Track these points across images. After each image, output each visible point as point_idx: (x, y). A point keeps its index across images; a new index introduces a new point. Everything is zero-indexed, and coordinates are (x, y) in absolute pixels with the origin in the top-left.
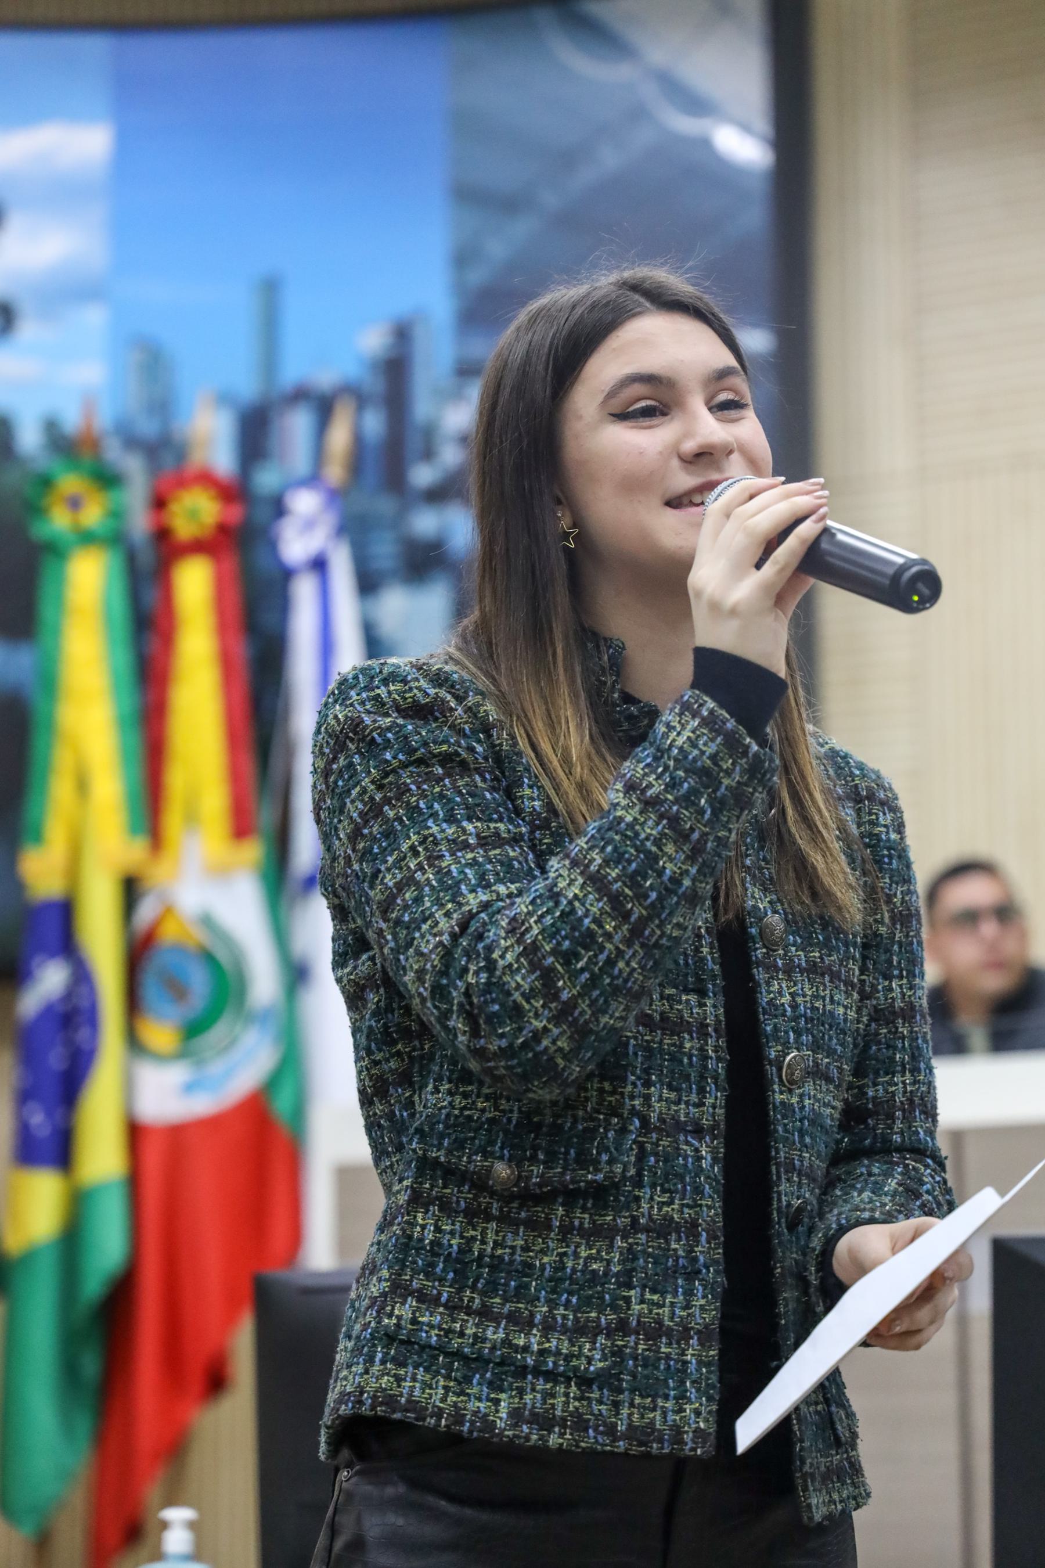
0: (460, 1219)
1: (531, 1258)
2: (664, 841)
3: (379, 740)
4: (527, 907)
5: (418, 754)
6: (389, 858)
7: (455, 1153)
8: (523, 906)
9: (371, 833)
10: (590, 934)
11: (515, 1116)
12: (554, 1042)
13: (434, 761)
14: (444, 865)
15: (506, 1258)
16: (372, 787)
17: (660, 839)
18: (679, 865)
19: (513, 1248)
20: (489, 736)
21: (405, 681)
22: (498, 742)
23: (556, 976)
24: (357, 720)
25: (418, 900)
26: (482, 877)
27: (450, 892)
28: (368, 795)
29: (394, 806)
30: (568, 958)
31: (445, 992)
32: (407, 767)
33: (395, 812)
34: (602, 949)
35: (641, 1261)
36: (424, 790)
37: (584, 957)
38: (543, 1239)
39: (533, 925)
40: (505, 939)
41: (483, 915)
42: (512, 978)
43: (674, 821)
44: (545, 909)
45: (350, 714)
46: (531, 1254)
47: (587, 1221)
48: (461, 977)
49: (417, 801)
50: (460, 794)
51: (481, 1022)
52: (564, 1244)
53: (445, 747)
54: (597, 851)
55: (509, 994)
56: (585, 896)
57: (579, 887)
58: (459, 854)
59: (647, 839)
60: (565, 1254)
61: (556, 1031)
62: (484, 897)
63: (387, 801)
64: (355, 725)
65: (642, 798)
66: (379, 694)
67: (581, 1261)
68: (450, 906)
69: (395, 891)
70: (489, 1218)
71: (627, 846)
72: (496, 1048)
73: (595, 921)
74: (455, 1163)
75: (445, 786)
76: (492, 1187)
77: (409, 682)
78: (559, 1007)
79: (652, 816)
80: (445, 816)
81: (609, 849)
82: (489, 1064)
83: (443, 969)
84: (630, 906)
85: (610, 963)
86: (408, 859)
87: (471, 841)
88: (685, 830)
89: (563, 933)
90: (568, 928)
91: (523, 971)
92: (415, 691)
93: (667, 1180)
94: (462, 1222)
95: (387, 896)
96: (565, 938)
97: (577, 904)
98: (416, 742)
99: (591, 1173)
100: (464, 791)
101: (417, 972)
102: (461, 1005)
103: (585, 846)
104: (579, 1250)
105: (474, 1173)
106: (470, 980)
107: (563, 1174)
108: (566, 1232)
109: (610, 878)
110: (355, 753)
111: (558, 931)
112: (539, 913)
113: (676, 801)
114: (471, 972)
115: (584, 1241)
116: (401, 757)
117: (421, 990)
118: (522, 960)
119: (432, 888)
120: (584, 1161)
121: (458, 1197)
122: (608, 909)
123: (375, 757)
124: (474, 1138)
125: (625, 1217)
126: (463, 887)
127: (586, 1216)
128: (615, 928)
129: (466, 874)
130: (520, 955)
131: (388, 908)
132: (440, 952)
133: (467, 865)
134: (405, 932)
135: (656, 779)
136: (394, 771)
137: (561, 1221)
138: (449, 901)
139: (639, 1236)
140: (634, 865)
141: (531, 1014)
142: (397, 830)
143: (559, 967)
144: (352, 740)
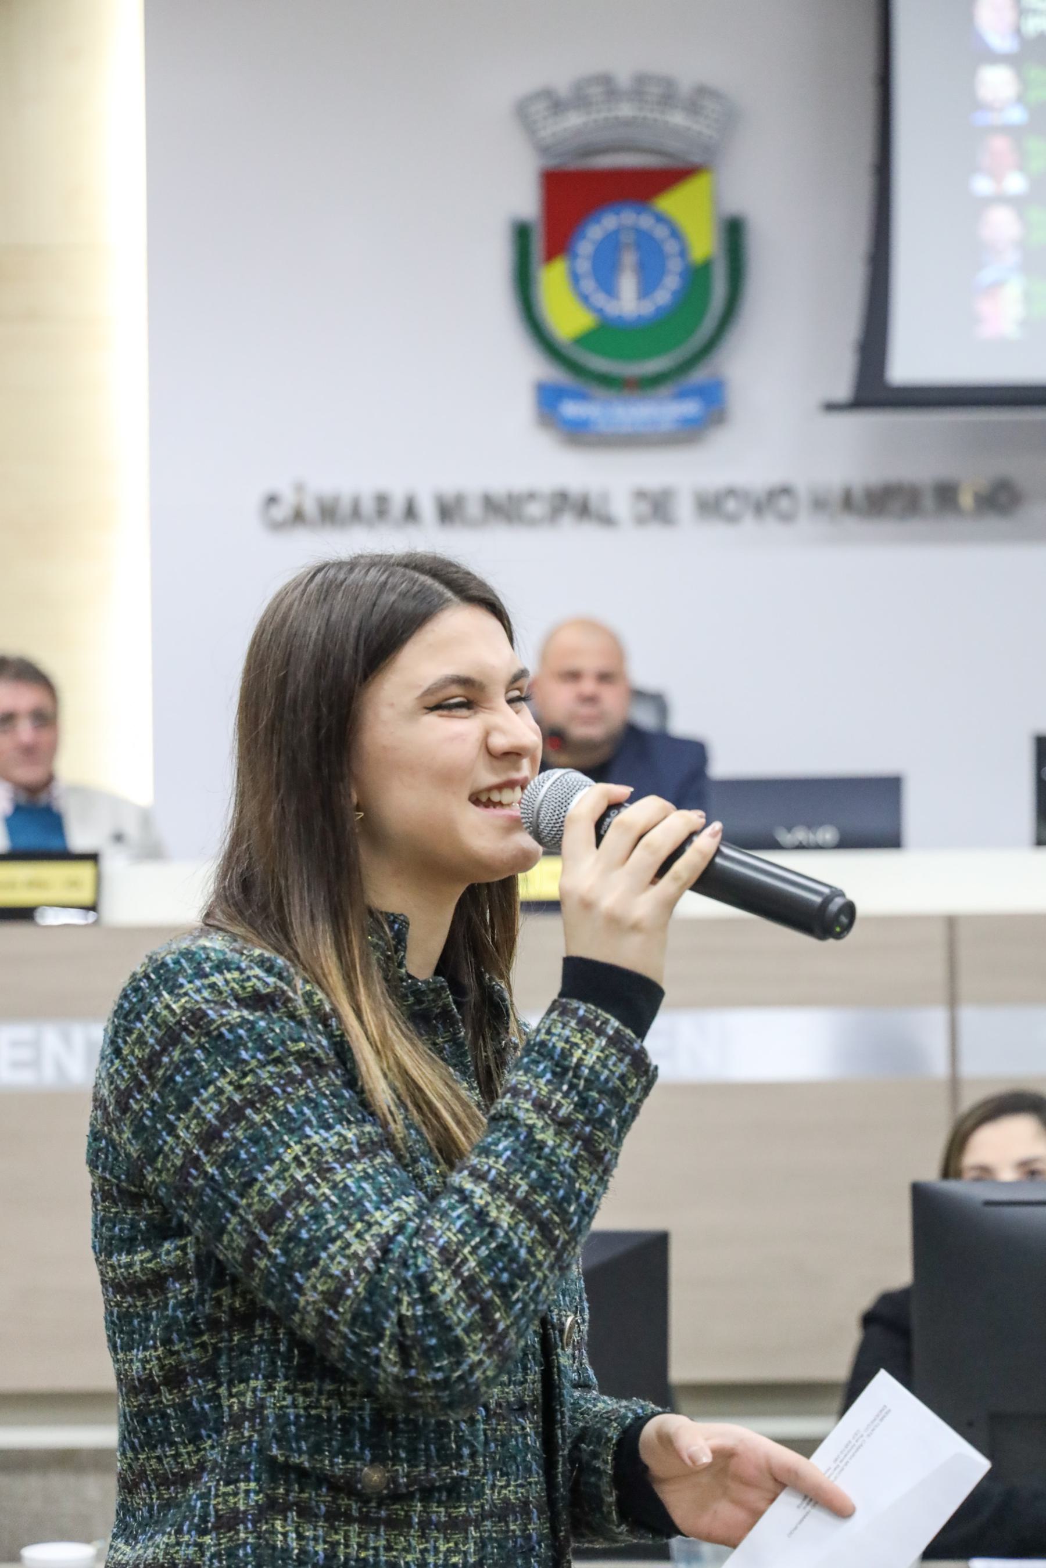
0: (321, 1524)
1: (395, 1557)
2: (580, 1163)
3: (229, 1036)
4: (455, 1235)
5: (277, 1053)
6: (267, 1168)
7: (316, 1457)
8: (449, 1234)
9: (235, 1139)
10: (526, 1265)
11: (367, 1413)
12: (484, 1372)
13: (291, 1059)
14: (338, 1178)
15: (371, 1560)
16: (230, 1088)
17: (576, 1161)
18: (593, 1187)
19: (376, 1549)
20: (326, 1026)
21: (242, 971)
22: (338, 1033)
23: (493, 1308)
24: (199, 1014)
25: (318, 1217)
26: (380, 1193)
27: (356, 1210)
28: (226, 1096)
29: (258, 1109)
30: (505, 1290)
31: (370, 1321)
32: (264, 1066)
33: (261, 1116)
34: (534, 1277)
35: (489, 1546)
36: (289, 1094)
37: (519, 1288)
38: (405, 1537)
39: (469, 1256)
40: (442, 1270)
41: (400, 1238)
42: (455, 1313)
43: (589, 1143)
44: (477, 1239)
45: (188, 1006)
46: (395, 1553)
47: (443, 1514)
48: (393, 1308)
49: (284, 1105)
50: (325, 1096)
51: (415, 1353)
52: (424, 1540)
53: (302, 1045)
54: (519, 1175)
55: (450, 1328)
56: (517, 1224)
57: (509, 1215)
58: (349, 1166)
59: (565, 1162)
60: (426, 1550)
61: (487, 1362)
62: (396, 1217)
63: (251, 1104)
64: (197, 1017)
65: (555, 1117)
66: (215, 984)
67: (441, 1556)
68: (359, 1226)
69: (280, 1203)
70: (349, 1520)
71: (553, 1171)
72: (429, 1380)
73: (531, 1251)
74: (320, 1468)
75: (308, 1087)
76: (361, 1490)
77: (245, 969)
78: (495, 1339)
79: (568, 1137)
80: (318, 1122)
81: (534, 1174)
82: (416, 1394)
83: (367, 1295)
84: (557, 1232)
85: (538, 1290)
86: (292, 1170)
87: (356, 1150)
88: (599, 1152)
89: (500, 1265)
90: (505, 1259)
91: (463, 1305)
92: (254, 980)
93: (505, 1464)
94: (323, 1527)
95: (271, 1209)
96: (503, 1270)
97: (511, 1234)
98: (273, 1040)
99: (456, 1469)
100: (328, 1092)
101: (322, 1292)
102: (392, 1336)
103: (504, 1169)
104: (437, 1544)
105: (342, 1477)
106: (404, 1311)
107: (427, 1471)
108: (425, 1525)
109: (538, 1205)
110: (196, 1048)
111: (495, 1263)
112: (473, 1243)
113: (587, 1122)
114: (405, 1303)
115: (442, 1535)
116: (260, 1056)
117: (331, 1313)
118: (461, 1293)
119: (334, 1205)
120: (446, 1457)
121: (317, 1502)
122: (539, 1237)
123: (226, 1055)
124: (331, 1439)
125: (477, 1507)
126: (368, 1205)
127: (442, 1509)
128: (545, 1256)
129: (363, 1189)
130: (459, 1288)
131: (274, 1221)
132: (364, 1278)
133: (361, 1177)
134: (303, 1250)
135: (564, 1097)
136: (252, 1071)
137: (420, 1517)
138: (356, 1221)
139: (486, 1523)
140: (561, 1192)
141: (470, 1348)
142: (266, 1136)
143: (497, 1300)
144: (191, 1034)
